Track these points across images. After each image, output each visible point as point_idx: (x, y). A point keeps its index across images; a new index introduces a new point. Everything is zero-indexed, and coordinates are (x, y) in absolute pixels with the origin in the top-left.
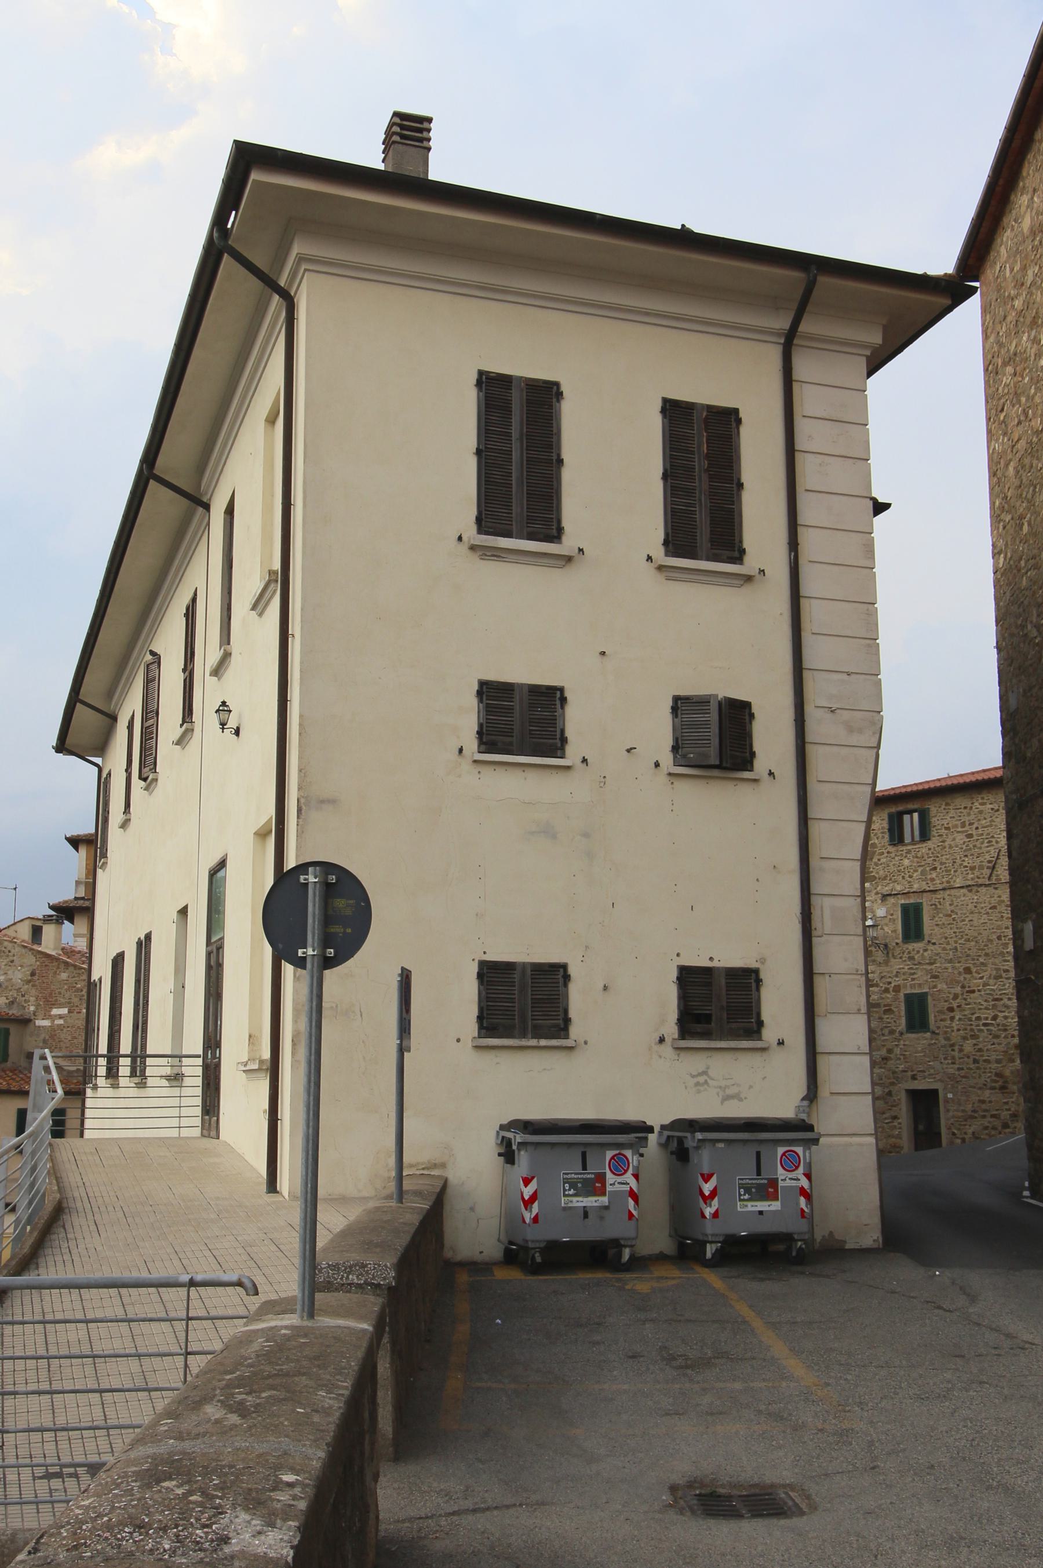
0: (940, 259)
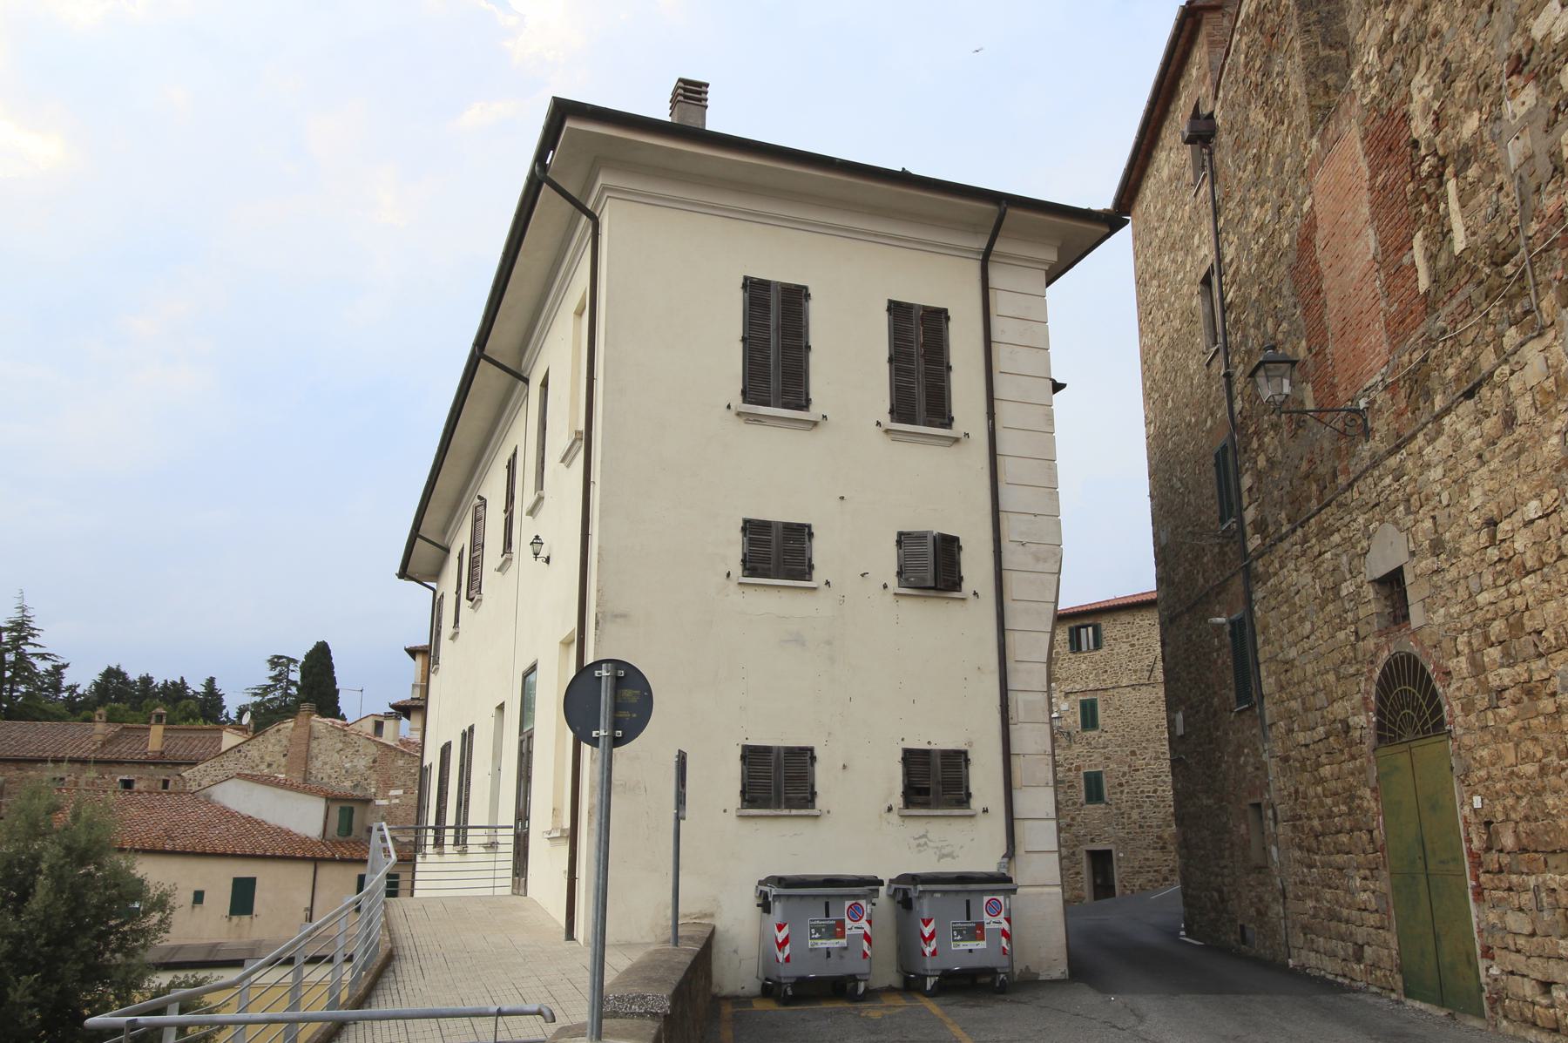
0: (1102, 198)
